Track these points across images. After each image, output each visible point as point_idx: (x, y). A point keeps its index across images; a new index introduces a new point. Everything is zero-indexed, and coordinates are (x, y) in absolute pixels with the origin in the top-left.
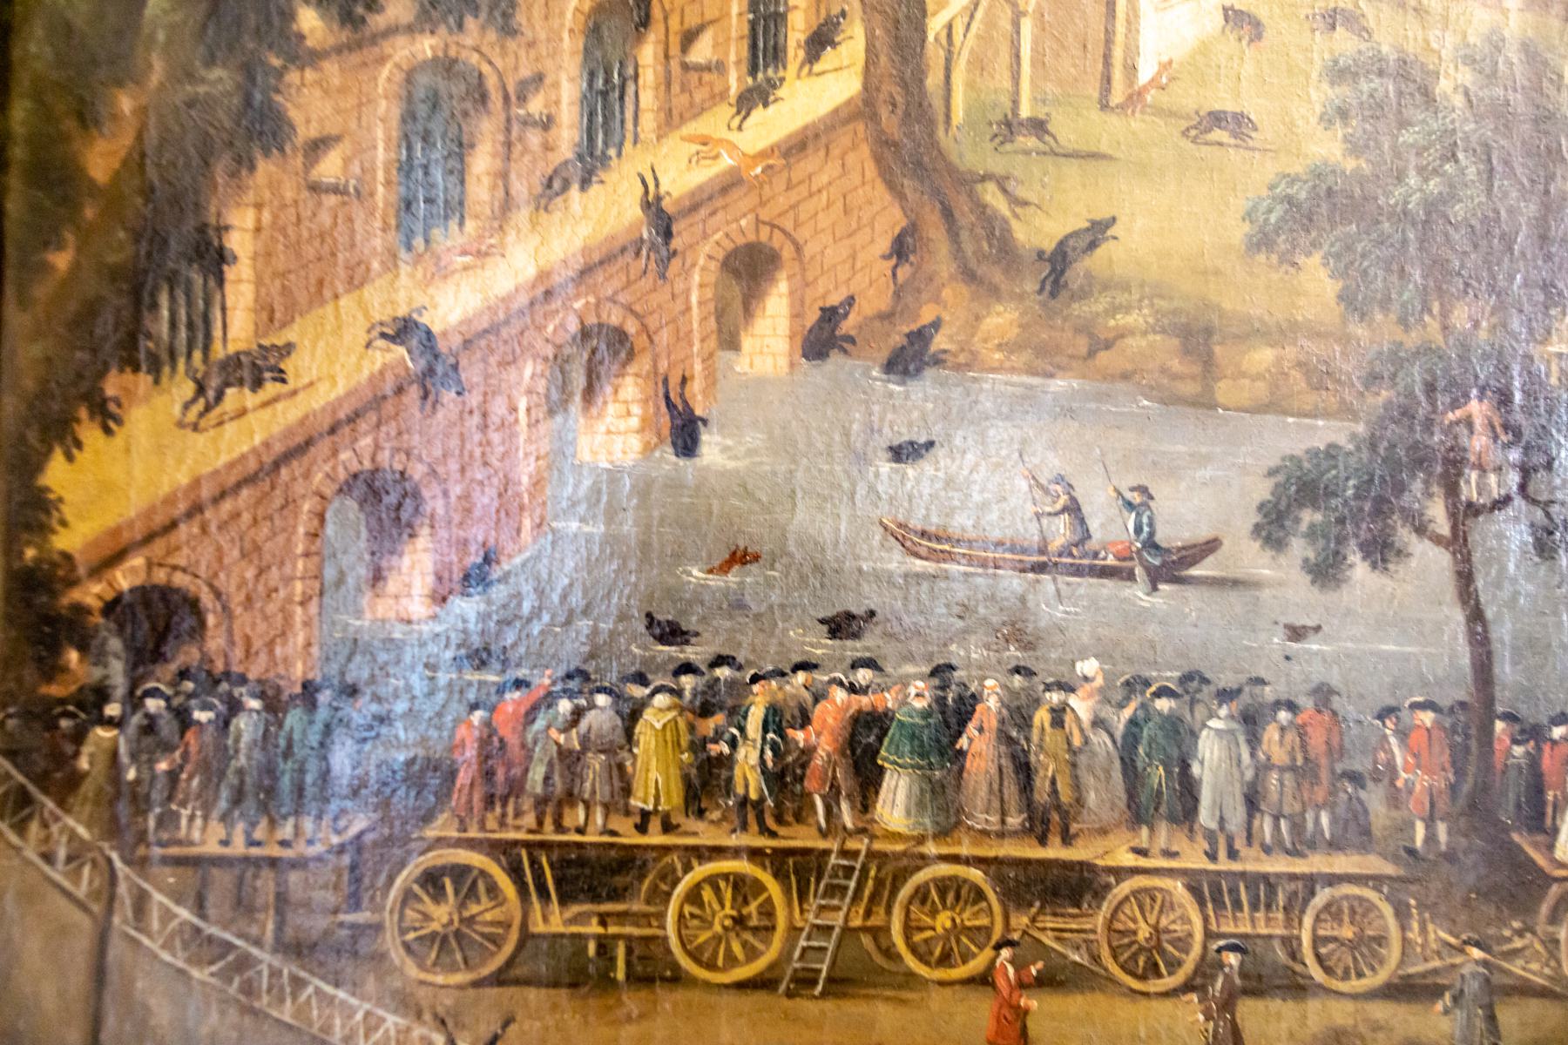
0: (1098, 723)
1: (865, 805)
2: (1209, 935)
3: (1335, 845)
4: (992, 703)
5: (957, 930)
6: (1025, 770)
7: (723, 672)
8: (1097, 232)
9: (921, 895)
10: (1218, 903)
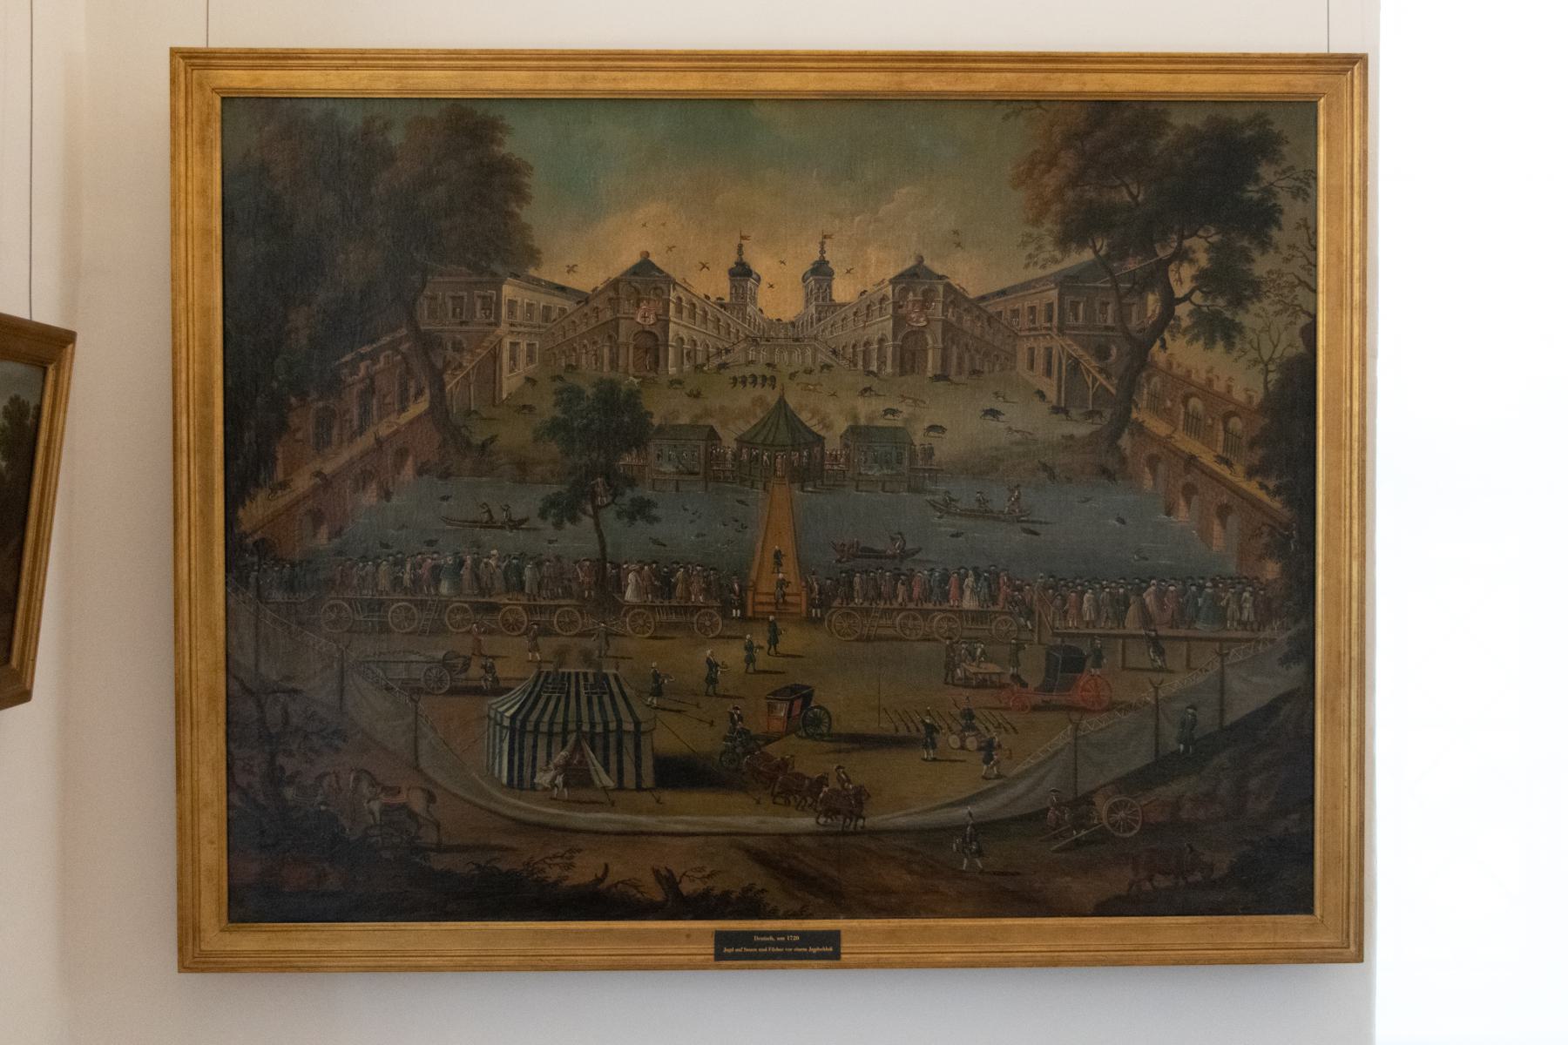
0: (498, 567)
1: (437, 589)
2: (528, 620)
3: (564, 598)
4: (469, 562)
7: (400, 556)
8: (493, 439)
9: (452, 611)
10: (532, 614)
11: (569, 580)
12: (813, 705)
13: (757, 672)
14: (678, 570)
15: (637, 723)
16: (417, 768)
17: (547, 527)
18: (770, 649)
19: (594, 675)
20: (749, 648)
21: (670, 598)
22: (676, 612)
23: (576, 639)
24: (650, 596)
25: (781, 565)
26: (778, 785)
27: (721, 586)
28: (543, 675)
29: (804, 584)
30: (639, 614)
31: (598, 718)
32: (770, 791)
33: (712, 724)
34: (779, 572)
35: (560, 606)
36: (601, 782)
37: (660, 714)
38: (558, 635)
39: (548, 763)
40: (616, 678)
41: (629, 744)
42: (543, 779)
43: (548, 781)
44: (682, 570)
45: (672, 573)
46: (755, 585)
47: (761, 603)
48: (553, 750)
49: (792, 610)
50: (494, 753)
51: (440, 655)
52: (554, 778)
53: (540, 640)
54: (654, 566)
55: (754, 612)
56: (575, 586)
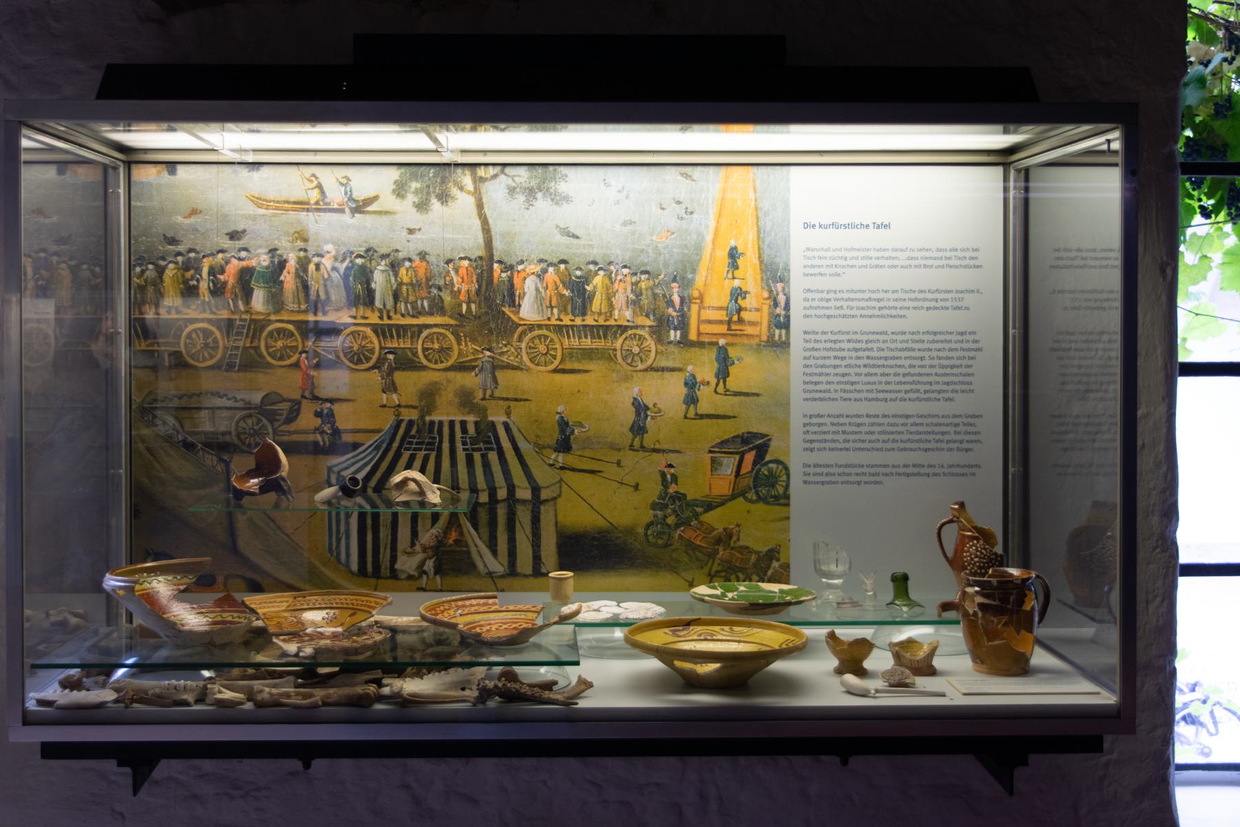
0: (334, 269)
2: (381, 348)
3: (431, 314)
5: (285, 347)
6: (306, 287)
7: (192, 255)
9: (271, 334)
10: (385, 337)
11: (440, 289)
12: (768, 458)
13: (702, 417)
14: (596, 274)
15: (536, 490)
16: (235, 550)
17: (405, 209)
18: (717, 385)
19: (476, 423)
20: (691, 384)
21: (584, 314)
22: (593, 337)
23: (451, 375)
24: (555, 311)
25: (737, 268)
26: (717, 561)
27: (655, 296)
28: (403, 426)
29: (766, 295)
30: (539, 337)
31: (481, 483)
32: (706, 570)
33: (636, 487)
34: (734, 278)
35: (427, 326)
36: (485, 566)
37: (568, 475)
38: (424, 368)
39: (413, 544)
40: (507, 427)
41: (524, 515)
42: (407, 564)
43: (414, 567)
44: (601, 273)
45: (586, 279)
46: (701, 297)
47: (710, 322)
48: (420, 528)
49: (749, 330)
50: (338, 531)
51: (257, 398)
52: (423, 563)
53: (399, 376)
54: (562, 266)
55: (699, 334)
56: (447, 298)
